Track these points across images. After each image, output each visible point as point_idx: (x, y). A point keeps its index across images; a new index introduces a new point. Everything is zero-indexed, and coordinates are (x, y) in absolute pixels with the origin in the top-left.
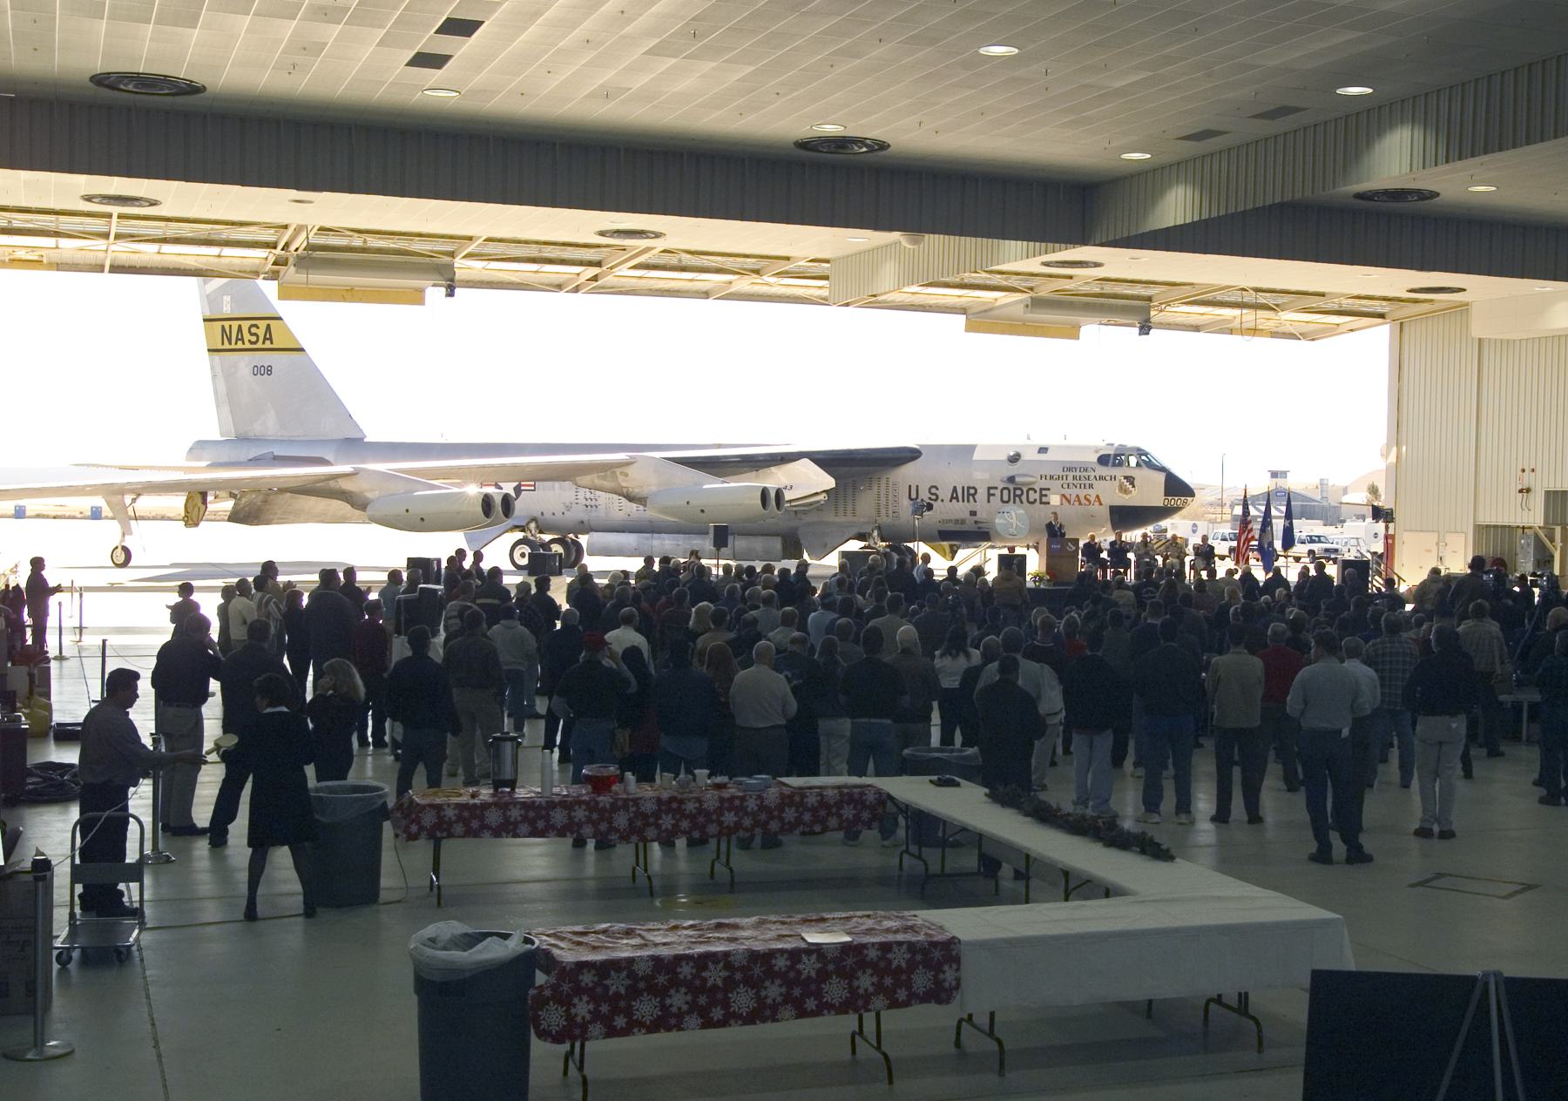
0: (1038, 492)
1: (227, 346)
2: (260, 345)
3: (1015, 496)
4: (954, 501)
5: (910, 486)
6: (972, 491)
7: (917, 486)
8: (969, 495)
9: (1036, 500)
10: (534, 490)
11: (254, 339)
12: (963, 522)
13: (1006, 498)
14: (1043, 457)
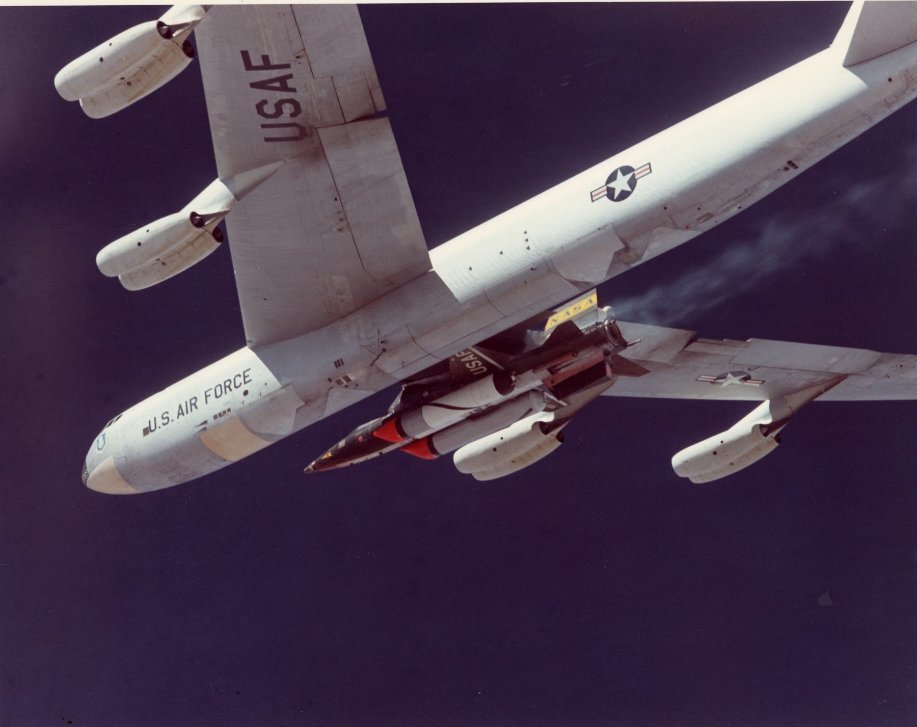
6: (193, 401)
7: (155, 419)
9: (241, 384)
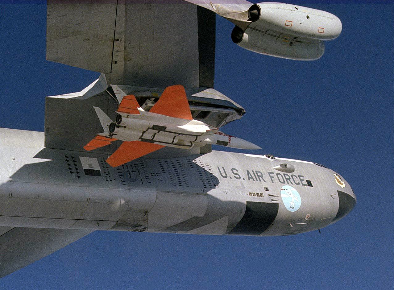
0: (298, 177)
3: (287, 179)
8: (259, 176)
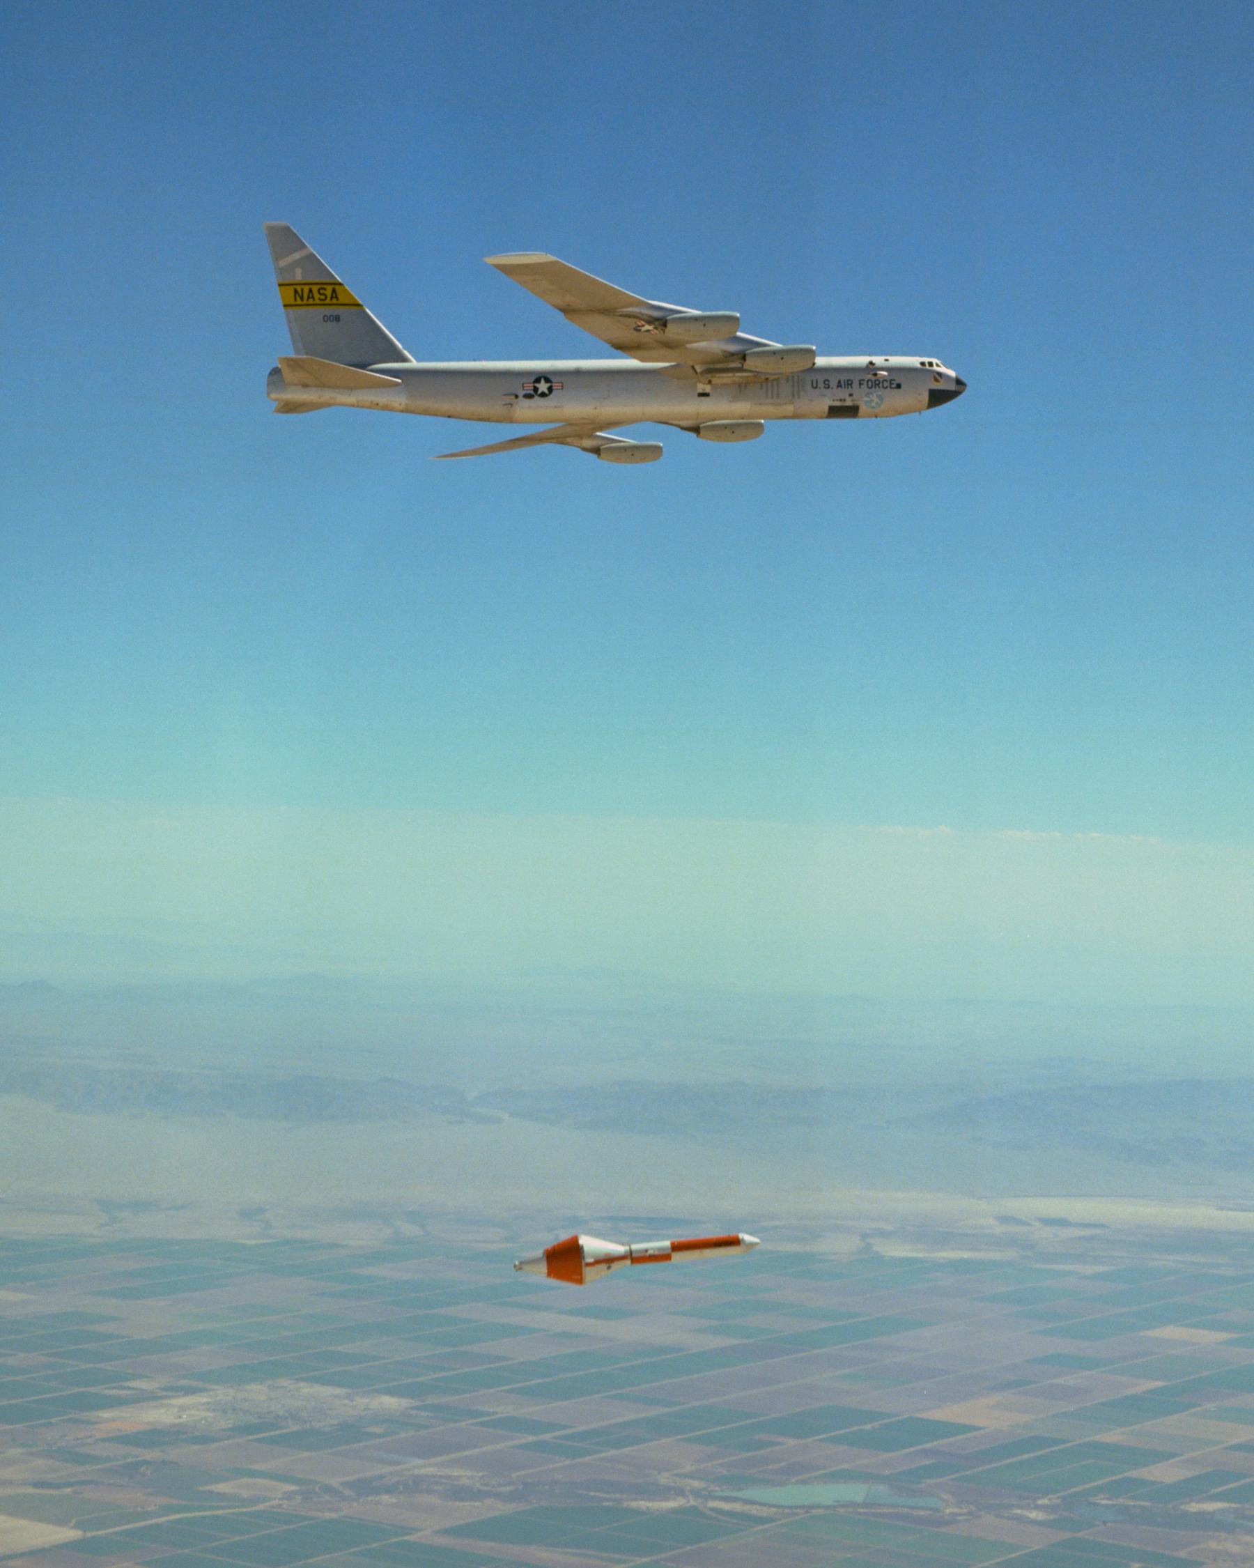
1: (299, 301)
2: (328, 301)
3: (876, 384)
4: (839, 388)
5: (812, 381)
6: (850, 382)
7: (817, 381)
8: (848, 384)
10: (562, 389)
11: (323, 297)
12: (845, 400)
13: (870, 385)
14: (887, 362)
